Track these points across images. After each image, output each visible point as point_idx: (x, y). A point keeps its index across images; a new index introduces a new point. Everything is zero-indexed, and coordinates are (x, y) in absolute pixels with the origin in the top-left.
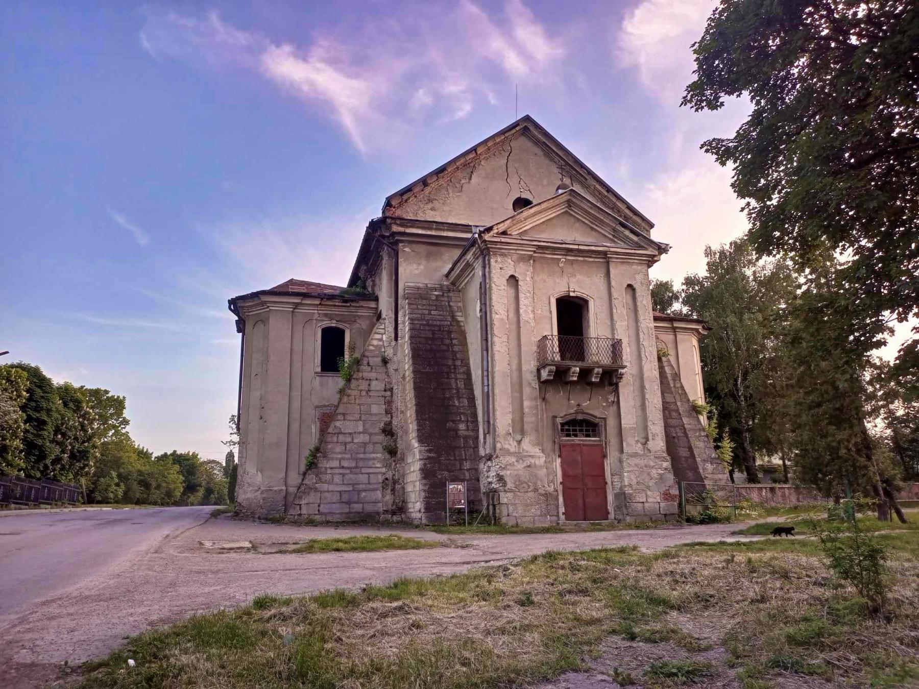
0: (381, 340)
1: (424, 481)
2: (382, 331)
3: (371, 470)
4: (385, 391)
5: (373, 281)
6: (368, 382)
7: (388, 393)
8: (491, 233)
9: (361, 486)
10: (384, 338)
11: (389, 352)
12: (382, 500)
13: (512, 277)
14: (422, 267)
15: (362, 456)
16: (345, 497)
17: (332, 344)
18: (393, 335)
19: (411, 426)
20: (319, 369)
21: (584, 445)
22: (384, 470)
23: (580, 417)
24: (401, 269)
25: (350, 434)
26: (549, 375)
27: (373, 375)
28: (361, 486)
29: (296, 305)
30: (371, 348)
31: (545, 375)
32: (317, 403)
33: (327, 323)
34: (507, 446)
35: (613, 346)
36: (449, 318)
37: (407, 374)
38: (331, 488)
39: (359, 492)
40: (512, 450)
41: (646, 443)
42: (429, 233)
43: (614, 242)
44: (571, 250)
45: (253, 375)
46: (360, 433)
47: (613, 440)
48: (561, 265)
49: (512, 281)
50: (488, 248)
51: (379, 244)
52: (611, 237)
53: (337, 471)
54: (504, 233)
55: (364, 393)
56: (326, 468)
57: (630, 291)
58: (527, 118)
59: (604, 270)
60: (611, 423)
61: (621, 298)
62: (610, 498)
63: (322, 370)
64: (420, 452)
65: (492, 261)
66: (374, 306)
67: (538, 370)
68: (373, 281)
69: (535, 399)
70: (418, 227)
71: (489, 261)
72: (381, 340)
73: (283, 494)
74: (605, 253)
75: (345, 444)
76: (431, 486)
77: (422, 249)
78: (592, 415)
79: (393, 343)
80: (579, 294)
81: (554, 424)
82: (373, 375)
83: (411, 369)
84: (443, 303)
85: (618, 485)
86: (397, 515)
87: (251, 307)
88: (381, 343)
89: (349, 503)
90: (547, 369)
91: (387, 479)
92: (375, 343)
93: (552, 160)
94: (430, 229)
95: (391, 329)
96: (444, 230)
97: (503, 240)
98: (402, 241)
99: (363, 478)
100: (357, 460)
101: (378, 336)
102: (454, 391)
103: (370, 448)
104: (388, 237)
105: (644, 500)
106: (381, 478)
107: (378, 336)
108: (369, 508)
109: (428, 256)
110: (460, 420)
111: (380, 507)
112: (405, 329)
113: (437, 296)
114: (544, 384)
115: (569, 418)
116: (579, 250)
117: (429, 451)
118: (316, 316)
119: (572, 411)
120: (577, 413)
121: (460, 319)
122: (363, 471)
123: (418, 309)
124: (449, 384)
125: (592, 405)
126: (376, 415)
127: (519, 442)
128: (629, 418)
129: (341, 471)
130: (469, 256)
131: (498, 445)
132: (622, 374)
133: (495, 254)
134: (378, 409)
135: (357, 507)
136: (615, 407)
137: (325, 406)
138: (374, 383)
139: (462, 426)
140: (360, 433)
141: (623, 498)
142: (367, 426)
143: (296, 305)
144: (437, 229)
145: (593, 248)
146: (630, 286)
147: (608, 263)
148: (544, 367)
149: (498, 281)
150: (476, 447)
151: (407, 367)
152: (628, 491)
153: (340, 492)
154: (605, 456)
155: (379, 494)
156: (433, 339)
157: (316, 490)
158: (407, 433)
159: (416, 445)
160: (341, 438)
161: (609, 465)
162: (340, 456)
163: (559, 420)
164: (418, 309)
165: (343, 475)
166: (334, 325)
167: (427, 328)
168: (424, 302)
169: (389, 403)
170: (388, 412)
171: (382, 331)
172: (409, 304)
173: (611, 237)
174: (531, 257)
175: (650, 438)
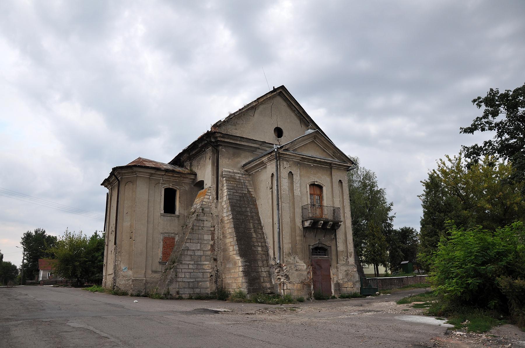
1: (245, 278)
2: (210, 194)
3: (203, 271)
5: (191, 163)
7: (212, 229)
8: (282, 149)
9: (199, 279)
12: (208, 287)
13: (290, 172)
15: (199, 263)
16: (191, 285)
17: (170, 197)
18: (215, 197)
19: (231, 248)
20: (163, 212)
22: (210, 271)
23: (320, 246)
24: (220, 161)
25: (193, 250)
27: (205, 218)
28: (199, 279)
29: (151, 175)
30: (204, 203)
31: (307, 224)
32: (161, 231)
33: (167, 186)
34: (289, 260)
35: (334, 210)
36: (246, 190)
37: (226, 218)
38: (185, 280)
39: (198, 282)
40: (292, 262)
41: (347, 259)
42: (236, 142)
43: (333, 158)
44: (316, 161)
45: (125, 214)
46: (198, 250)
47: (334, 257)
49: (290, 174)
50: (280, 157)
51: (206, 146)
53: (186, 271)
54: (287, 150)
55: (200, 228)
56: (182, 269)
57: (340, 184)
58: (283, 87)
59: (329, 172)
60: (333, 248)
61: (336, 185)
64: (242, 262)
66: (193, 178)
67: (303, 222)
68: (191, 163)
69: (301, 236)
70: (231, 139)
71: (280, 163)
73: (144, 282)
74: (331, 164)
75: (191, 255)
76: (249, 280)
77: (231, 151)
79: (215, 201)
80: (319, 184)
81: (309, 248)
82: (205, 218)
83: (231, 217)
84: (242, 181)
85: (335, 279)
86: (221, 295)
87: (125, 173)
89: (193, 288)
90: (309, 222)
91: (212, 276)
92: (205, 200)
93: (292, 109)
94: (237, 140)
95: (214, 193)
97: (288, 153)
98: (221, 145)
99: (200, 275)
100: (197, 264)
103: (203, 258)
104: (214, 142)
106: (209, 275)
108: (203, 291)
111: (209, 291)
112: (225, 193)
114: (305, 228)
115: (315, 246)
116: (320, 161)
117: (246, 262)
118: (161, 181)
119: (317, 243)
120: (319, 244)
121: (251, 190)
122: (200, 271)
125: (325, 241)
127: (294, 258)
128: (341, 247)
129: (189, 271)
130: (265, 159)
131: (285, 259)
132: (340, 225)
133: (283, 160)
134: (207, 237)
135: (197, 291)
136: (334, 241)
138: (206, 222)
139: (260, 249)
140: (198, 250)
141: (338, 286)
142: (202, 246)
143: (151, 175)
144: (240, 141)
145: (326, 161)
146: (340, 181)
147: (331, 168)
148: (307, 220)
149: (284, 173)
150: (267, 260)
152: (341, 282)
153: (189, 282)
154: (331, 266)
155: (208, 284)
156: (240, 200)
157: (177, 282)
158: (225, 250)
159: (239, 258)
160: (189, 253)
161: (332, 271)
162: (188, 262)
163: (311, 247)
165: (190, 273)
167: (237, 194)
169: (213, 234)
170: (213, 239)
171: (210, 194)
172: (226, 180)
174: (299, 163)
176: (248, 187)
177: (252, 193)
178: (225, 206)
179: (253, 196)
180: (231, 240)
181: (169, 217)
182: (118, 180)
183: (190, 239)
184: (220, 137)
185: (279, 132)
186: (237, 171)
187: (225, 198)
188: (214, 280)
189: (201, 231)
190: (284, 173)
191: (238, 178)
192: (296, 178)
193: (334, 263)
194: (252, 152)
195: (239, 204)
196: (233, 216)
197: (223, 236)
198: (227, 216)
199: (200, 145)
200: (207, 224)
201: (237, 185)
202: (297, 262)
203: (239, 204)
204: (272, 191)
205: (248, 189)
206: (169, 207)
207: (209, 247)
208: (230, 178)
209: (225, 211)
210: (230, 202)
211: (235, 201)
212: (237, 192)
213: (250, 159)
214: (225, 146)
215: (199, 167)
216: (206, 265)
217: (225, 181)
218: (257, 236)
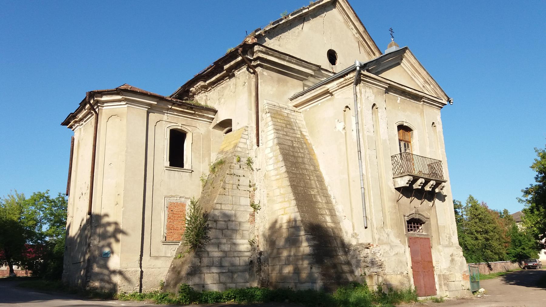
0: (246, 143)
4: (250, 186)
6: (238, 178)
10: (248, 143)
11: (252, 155)
14: (275, 89)
18: (255, 140)
20: (168, 164)
21: (421, 238)
23: (417, 217)
26: (407, 183)
27: (241, 172)
30: (239, 149)
31: (403, 182)
34: (382, 238)
48: (398, 101)
51: (238, 66)
52: (421, 86)
55: (235, 187)
62: (436, 279)
63: (170, 166)
65: (363, 90)
72: (246, 143)
78: (423, 216)
83: (284, 169)
84: (292, 120)
88: (246, 146)
93: (348, 26)
94: (284, 60)
96: (293, 63)
101: (244, 141)
102: (316, 191)
105: (454, 280)
107: (244, 141)
109: (279, 81)
110: (326, 214)
113: (288, 114)
115: (411, 217)
117: (313, 239)
119: (413, 212)
121: (304, 133)
123: (278, 122)
124: (311, 184)
126: (244, 206)
130: (331, 86)
137: (172, 196)
138: (242, 179)
149: (365, 106)
151: (271, 167)
163: (407, 219)
164: (278, 122)
166: (180, 128)
167: (287, 138)
168: (280, 117)
169: (252, 197)
173: (421, 86)
175: (452, 235)
176: (302, 130)
177: (307, 138)
178: (271, 155)
179: (309, 141)
180: (286, 205)
181: (176, 173)
182: (96, 112)
183: (221, 204)
184: (261, 52)
185: (332, 56)
186: (283, 106)
187: (270, 144)
188: (255, 269)
189: (236, 191)
190: (365, 106)
191: (286, 115)
192: (381, 113)
193: (434, 243)
194: (301, 80)
195: (293, 152)
196: (287, 168)
197: (269, 201)
198: (276, 169)
199: (226, 67)
200: (244, 182)
201: (286, 124)
202: (391, 241)
203: (293, 152)
204: (346, 133)
205: (301, 132)
206: (176, 159)
207: (248, 216)
208: (276, 113)
209: (271, 161)
210: (280, 149)
211: (286, 147)
212: (287, 135)
213: (300, 90)
214: (267, 68)
215: (223, 100)
216: (243, 244)
217: (270, 119)
218: (322, 199)
